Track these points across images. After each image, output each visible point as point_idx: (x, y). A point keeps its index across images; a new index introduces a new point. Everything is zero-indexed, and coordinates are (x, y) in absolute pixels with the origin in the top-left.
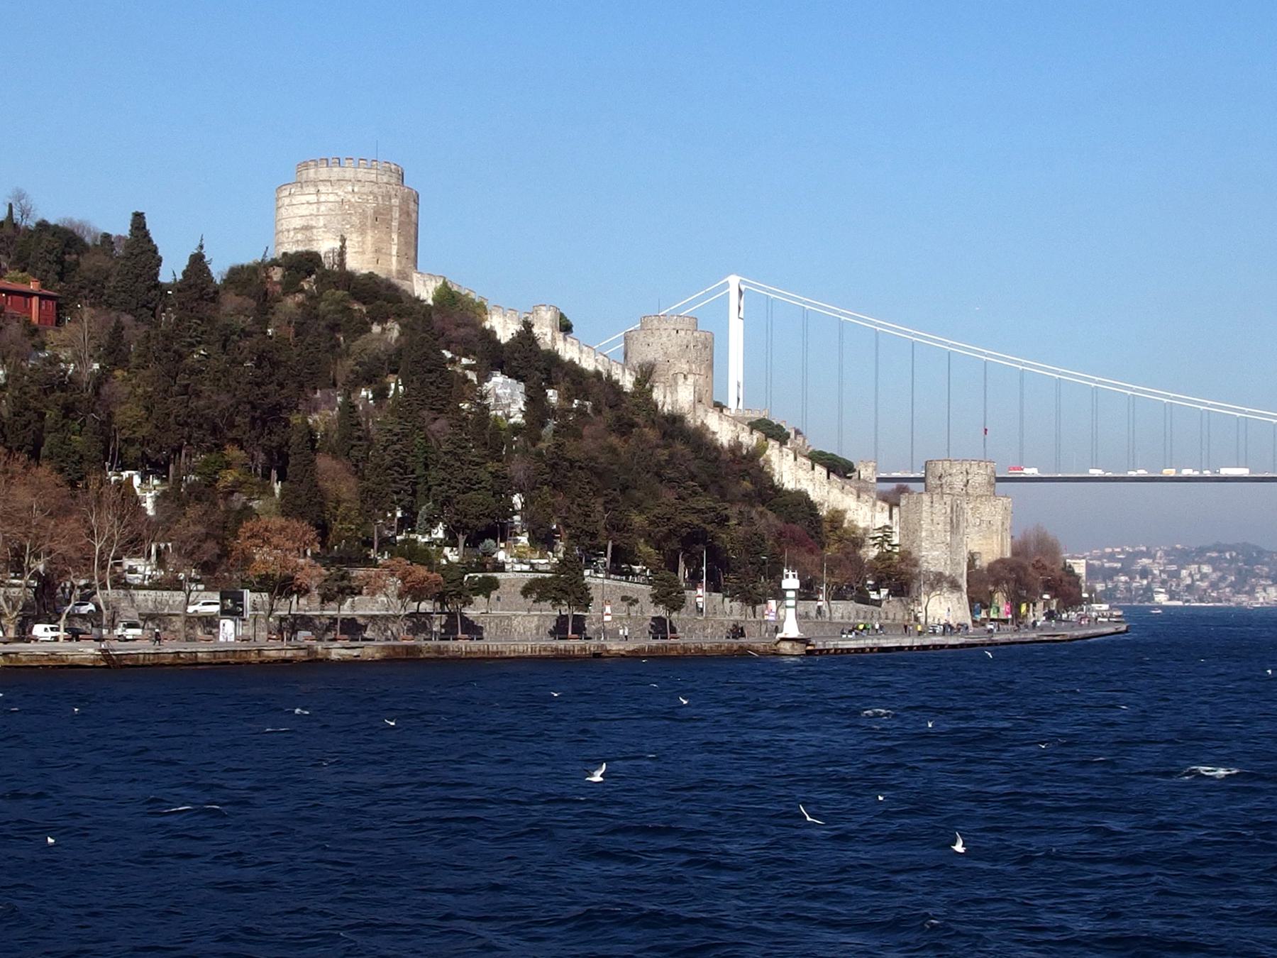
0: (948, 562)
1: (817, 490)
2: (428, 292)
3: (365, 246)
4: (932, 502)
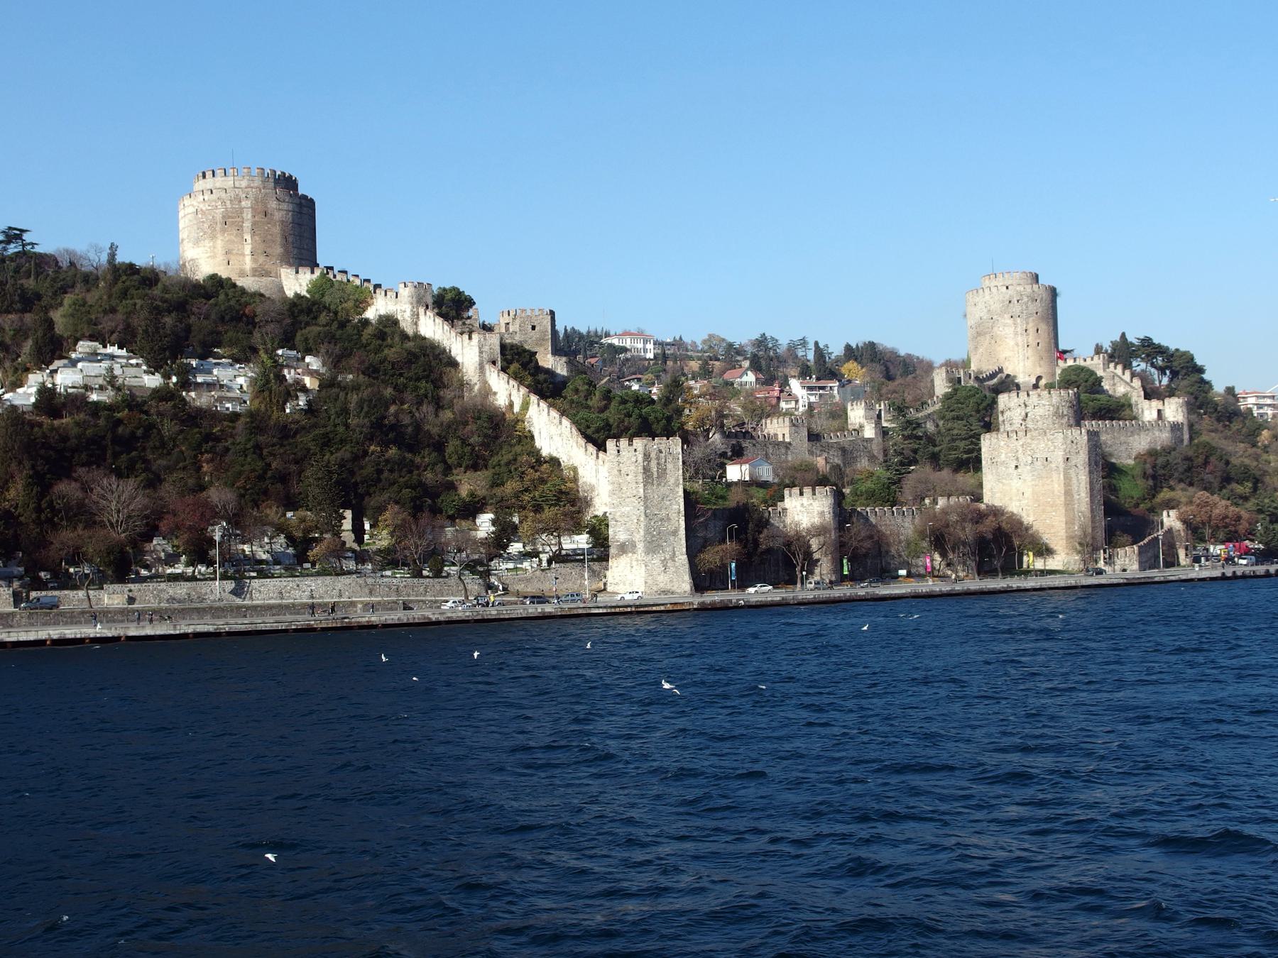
0: (642, 519)
1: (565, 445)
2: (300, 285)
3: (216, 250)
4: (619, 451)
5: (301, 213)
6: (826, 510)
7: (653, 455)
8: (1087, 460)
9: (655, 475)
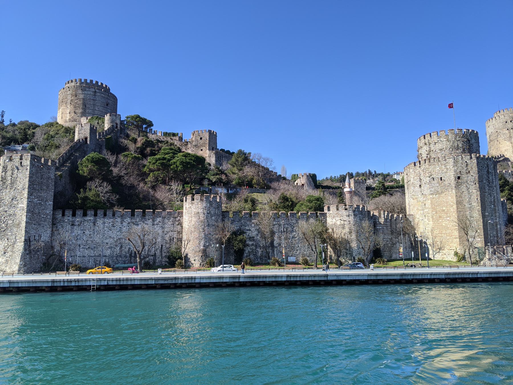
6: (200, 211)
7: (9, 168)
8: (477, 178)
9: (9, 182)
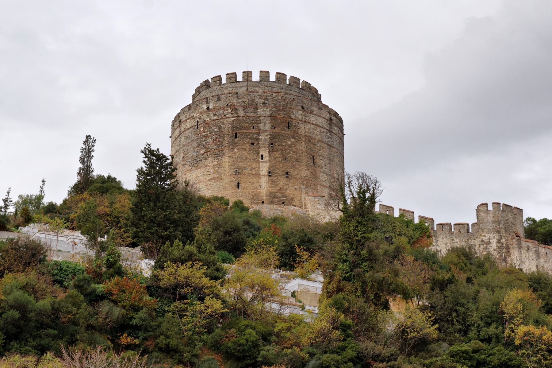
5: (330, 131)
